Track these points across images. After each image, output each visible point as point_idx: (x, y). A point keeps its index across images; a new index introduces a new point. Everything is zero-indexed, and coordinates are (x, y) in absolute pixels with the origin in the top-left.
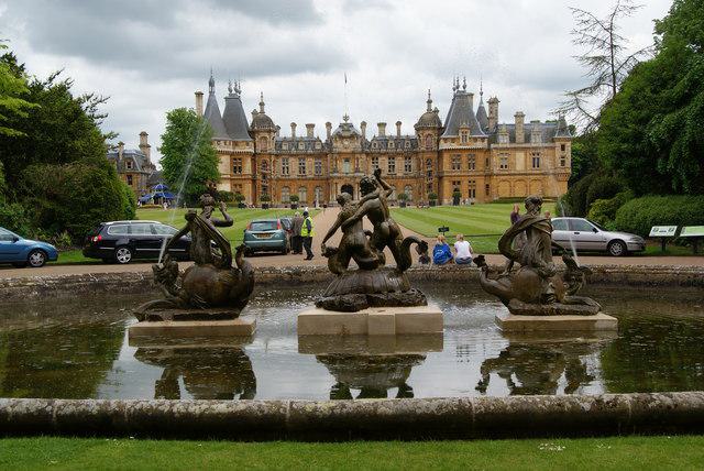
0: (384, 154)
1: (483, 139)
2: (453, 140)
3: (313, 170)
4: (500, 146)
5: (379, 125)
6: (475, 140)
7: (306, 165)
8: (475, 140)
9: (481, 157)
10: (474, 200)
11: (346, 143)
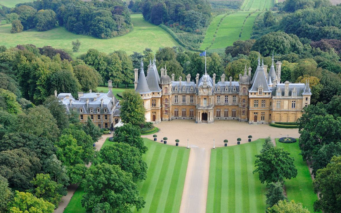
0: (223, 94)
1: (269, 93)
2: (255, 94)
4: (277, 97)
6: (266, 93)
7: (186, 99)
9: (268, 102)
10: (263, 121)
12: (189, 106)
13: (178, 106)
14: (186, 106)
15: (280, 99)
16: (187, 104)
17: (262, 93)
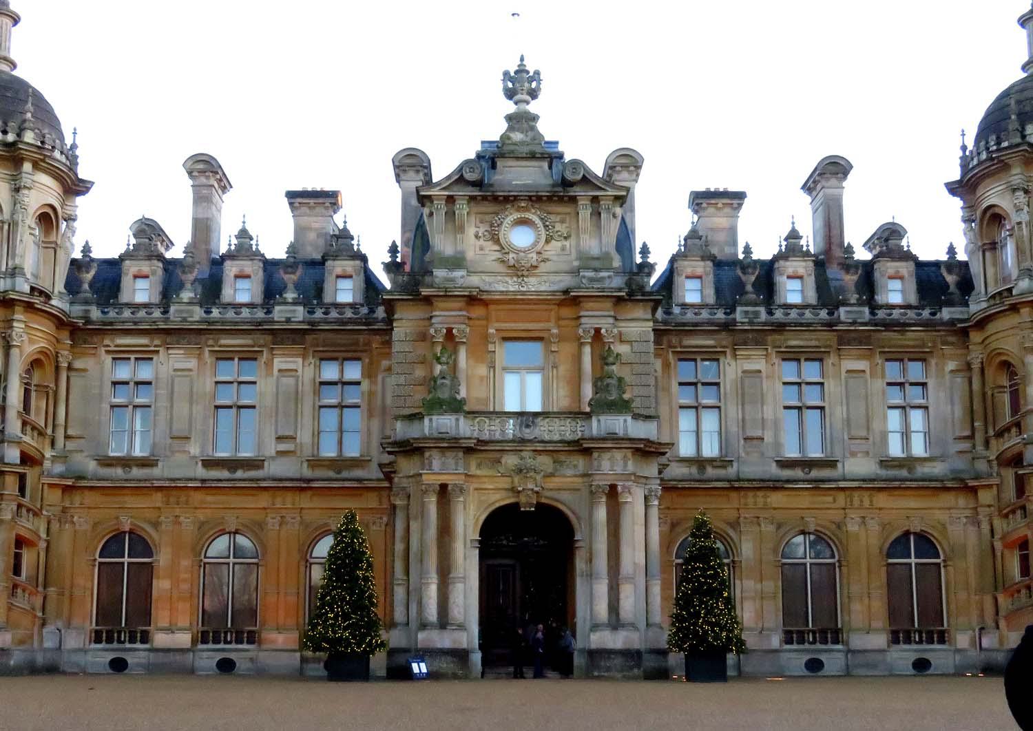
3: (305, 436)
5: (701, 200)
11: (521, 238)
12: (302, 486)
13: (142, 489)
14: (257, 488)
16: (276, 468)
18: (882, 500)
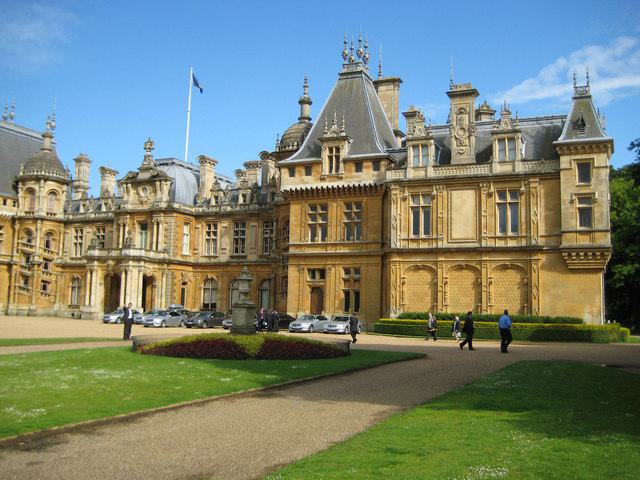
2: (308, 169)
8: (359, 165)
15: (427, 183)
17: (341, 165)
18: (259, 269)
